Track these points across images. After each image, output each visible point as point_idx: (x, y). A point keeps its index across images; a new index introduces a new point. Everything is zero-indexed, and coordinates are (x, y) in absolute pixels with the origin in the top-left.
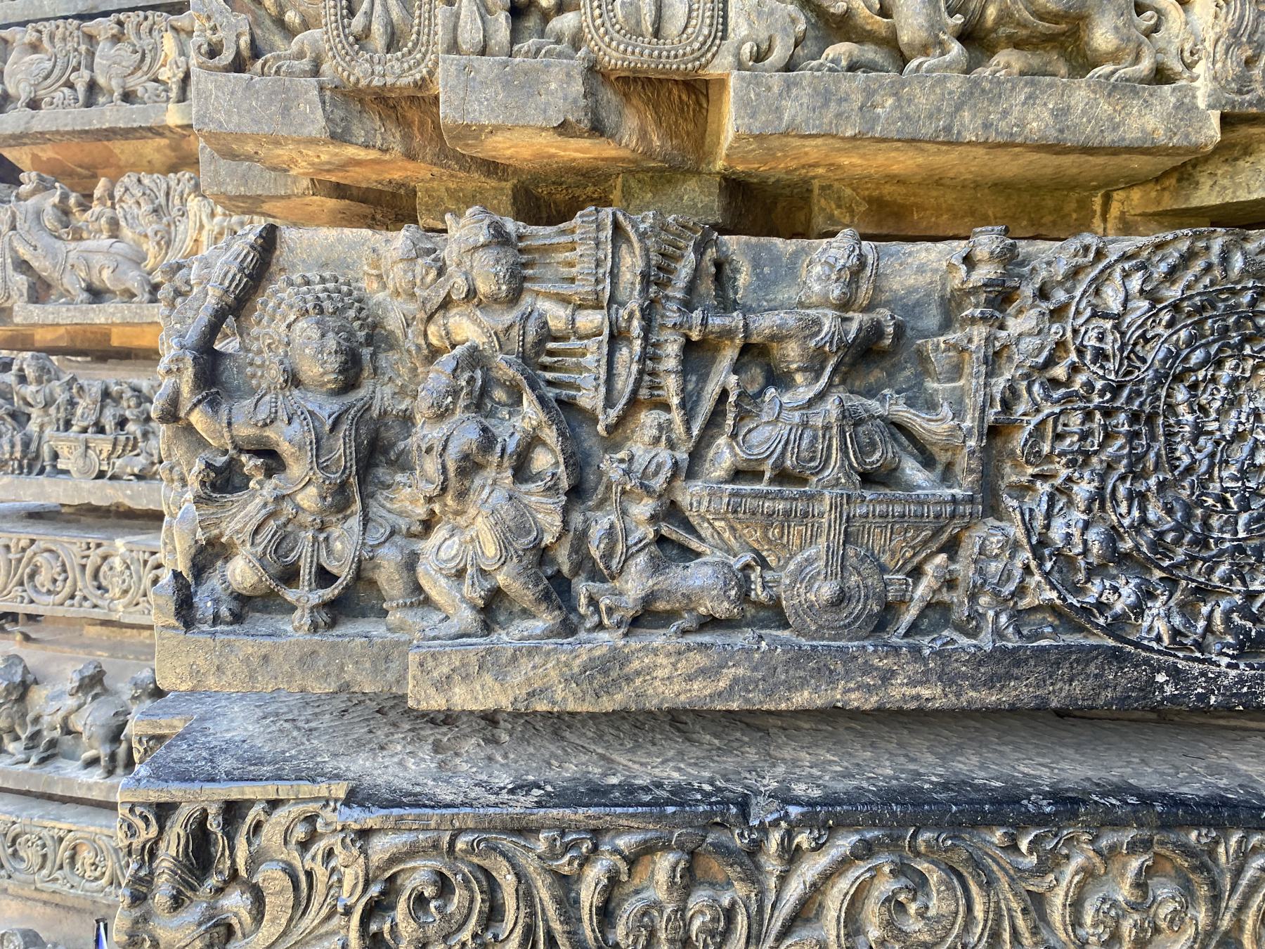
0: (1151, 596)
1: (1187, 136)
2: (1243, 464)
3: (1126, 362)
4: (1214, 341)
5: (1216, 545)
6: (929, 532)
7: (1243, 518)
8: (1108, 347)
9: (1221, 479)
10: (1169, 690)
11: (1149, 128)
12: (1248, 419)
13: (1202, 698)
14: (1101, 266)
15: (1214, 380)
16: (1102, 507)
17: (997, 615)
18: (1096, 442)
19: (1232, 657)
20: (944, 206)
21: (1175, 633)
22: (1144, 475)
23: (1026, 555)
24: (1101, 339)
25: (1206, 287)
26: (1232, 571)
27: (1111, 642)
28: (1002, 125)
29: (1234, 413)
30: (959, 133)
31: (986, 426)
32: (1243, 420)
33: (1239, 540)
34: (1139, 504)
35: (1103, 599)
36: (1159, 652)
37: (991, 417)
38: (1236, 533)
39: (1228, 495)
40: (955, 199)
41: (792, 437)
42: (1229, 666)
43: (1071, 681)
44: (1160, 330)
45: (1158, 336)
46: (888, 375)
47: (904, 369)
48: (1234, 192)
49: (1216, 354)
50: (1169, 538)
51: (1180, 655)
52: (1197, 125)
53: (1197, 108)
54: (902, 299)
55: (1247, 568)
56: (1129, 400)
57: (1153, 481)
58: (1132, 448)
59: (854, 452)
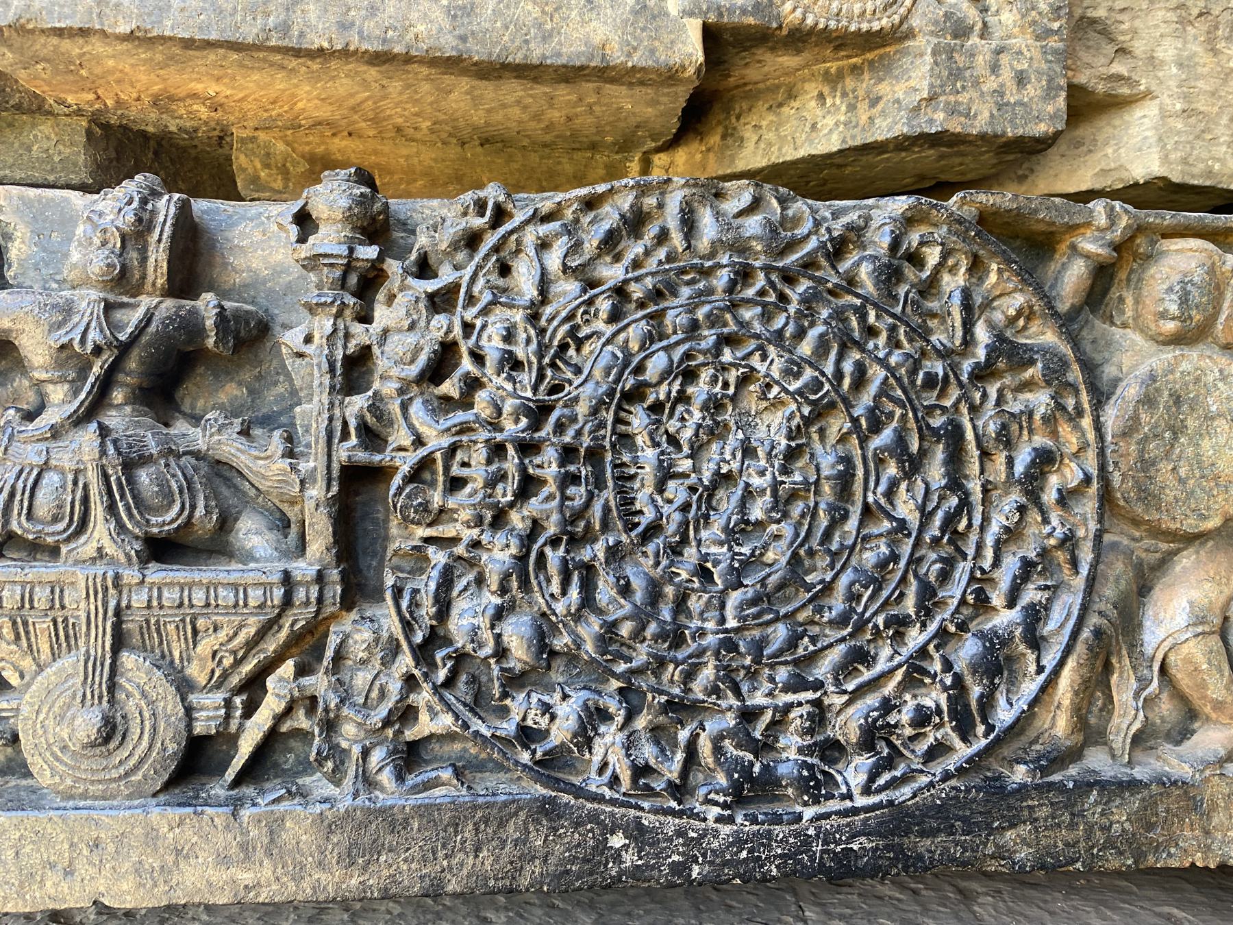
0: (604, 715)
1: (652, 51)
2: (729, 518)
3: (549, 373)
4: (678, 343)
5: (693, 638)
6: (252, 631)
7: (735, 597)
8: (520, 352)
9: (699, 543)
10: (629, 858)
11: (597, 39)
12: (734, 455)
13: (680, 869)
14: (502, 231)
15: (683, 398)
16: (525, 584)
17: (366, 753)
18: (509, 489)
19: (725, 806)
20: (418, 168)
21: (641, 771)
22: (588, 537)
23: (405, 661)
24: (509, 337)
25: (660, 262)
26: (718, 678)
27: (540, 790)
28: (369, 26)
29: (715, 447)
30: (302, 35)
31: (336, 466)
32: (728, 457)
33: (727, 631)
34: (582, 579)
35: (529, 723)
36: (613, 802)
37: (343, 453)
38: (722, 620)
39: (709, 565)
40: (435, 160)
41: (20, 485)
42: (719, 820)
43: (477, 850)
44: (600, 325)
45: (597, 334)
46: (251, 392)
47: (276, 383)
48: (780, 149)
49: (681, 361)
50: (625, 630)
51: (646, 805)
52: (667, 38)
53: (667, 14)
54: (264, 283)
55: (742, 673)
56: (560, 428)
57: (599, 549)
58: (564, 498)
59: (128, 509)
